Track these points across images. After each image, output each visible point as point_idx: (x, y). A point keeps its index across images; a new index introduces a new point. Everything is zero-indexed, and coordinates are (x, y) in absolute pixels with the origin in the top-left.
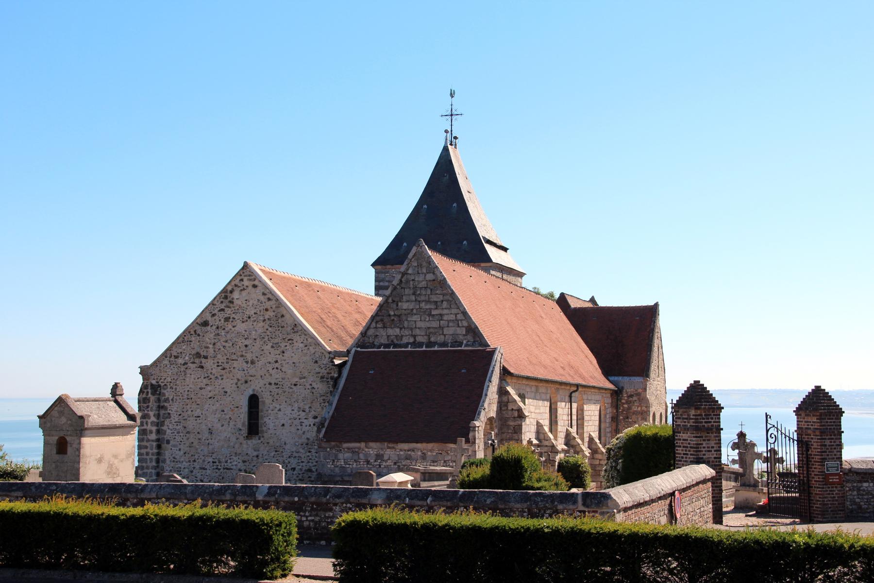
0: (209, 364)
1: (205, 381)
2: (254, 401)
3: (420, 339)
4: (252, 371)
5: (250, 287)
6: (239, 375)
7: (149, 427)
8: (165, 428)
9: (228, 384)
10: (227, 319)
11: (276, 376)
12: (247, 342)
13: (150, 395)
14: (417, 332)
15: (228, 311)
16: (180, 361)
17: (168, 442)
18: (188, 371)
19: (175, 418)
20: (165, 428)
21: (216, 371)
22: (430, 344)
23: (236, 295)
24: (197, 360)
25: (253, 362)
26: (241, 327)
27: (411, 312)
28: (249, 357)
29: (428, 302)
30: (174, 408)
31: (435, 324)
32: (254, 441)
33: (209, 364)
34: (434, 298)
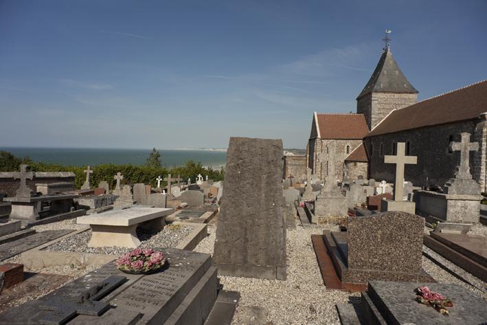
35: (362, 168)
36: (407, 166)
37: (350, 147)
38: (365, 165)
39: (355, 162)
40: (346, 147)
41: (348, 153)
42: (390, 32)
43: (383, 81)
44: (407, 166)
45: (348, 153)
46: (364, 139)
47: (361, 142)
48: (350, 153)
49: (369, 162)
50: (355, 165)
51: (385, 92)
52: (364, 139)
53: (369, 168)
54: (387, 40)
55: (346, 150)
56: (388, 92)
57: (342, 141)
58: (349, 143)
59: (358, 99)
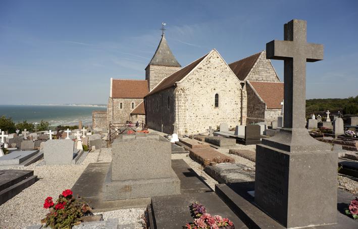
0: (202, 82)
1: (201, 88)
2: (217, 96)
3: (264, 79)
4: (216, 86)
5: (216, 58)
6: (213, 87)
7: (182, 104)
8: (186, 105)
9: (209, 90)
10: (208, 68)
11: (224, 88)
12: (215, 76)
13: (182, 93)
14: (263, 77)
15: (209, 65)
16: (192, 81)
17: (187, 110)
18: (195, 85)
19: (189, 101)
20: (186, 105)
21: (205, 85)
22: (267, 81)
23: (211, 60)
24: (198, 81)
25: (217, 83)
26: (213, 71)
27: (262, 71)
28: (216, 81)
29: (266, 68)
30: (189, 98)
31: (268, 75)
32: (217, 109)
33: (202, 82)
34: (268, 67)
35: (141, 119)
36: (69, 133)
37: (135, 104)
38: (144, 117)
39: (137, 114)
40: (131, 104)
41: (133, 108)
42: (165, 24)
43: (159, 58)
44: (69, 133)
45: (133, 108)
46: (144, 98)
47: (142, 101)
48: (135, 108)
49: (146, 115)
50: (137, 117)
51: (159, 65)
52: (144, 98)
53: (146, 119)
54: (163, 29)
55: (131, 106)
56: (161, 65)
57: (128, 100)
58: (134, 101)
59: (145, 69)
